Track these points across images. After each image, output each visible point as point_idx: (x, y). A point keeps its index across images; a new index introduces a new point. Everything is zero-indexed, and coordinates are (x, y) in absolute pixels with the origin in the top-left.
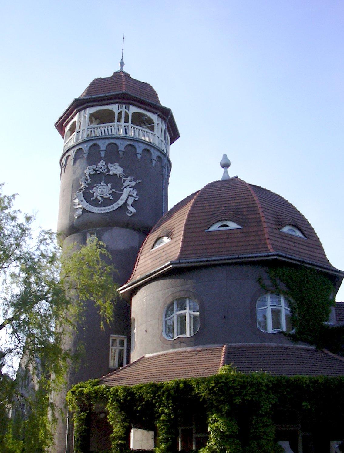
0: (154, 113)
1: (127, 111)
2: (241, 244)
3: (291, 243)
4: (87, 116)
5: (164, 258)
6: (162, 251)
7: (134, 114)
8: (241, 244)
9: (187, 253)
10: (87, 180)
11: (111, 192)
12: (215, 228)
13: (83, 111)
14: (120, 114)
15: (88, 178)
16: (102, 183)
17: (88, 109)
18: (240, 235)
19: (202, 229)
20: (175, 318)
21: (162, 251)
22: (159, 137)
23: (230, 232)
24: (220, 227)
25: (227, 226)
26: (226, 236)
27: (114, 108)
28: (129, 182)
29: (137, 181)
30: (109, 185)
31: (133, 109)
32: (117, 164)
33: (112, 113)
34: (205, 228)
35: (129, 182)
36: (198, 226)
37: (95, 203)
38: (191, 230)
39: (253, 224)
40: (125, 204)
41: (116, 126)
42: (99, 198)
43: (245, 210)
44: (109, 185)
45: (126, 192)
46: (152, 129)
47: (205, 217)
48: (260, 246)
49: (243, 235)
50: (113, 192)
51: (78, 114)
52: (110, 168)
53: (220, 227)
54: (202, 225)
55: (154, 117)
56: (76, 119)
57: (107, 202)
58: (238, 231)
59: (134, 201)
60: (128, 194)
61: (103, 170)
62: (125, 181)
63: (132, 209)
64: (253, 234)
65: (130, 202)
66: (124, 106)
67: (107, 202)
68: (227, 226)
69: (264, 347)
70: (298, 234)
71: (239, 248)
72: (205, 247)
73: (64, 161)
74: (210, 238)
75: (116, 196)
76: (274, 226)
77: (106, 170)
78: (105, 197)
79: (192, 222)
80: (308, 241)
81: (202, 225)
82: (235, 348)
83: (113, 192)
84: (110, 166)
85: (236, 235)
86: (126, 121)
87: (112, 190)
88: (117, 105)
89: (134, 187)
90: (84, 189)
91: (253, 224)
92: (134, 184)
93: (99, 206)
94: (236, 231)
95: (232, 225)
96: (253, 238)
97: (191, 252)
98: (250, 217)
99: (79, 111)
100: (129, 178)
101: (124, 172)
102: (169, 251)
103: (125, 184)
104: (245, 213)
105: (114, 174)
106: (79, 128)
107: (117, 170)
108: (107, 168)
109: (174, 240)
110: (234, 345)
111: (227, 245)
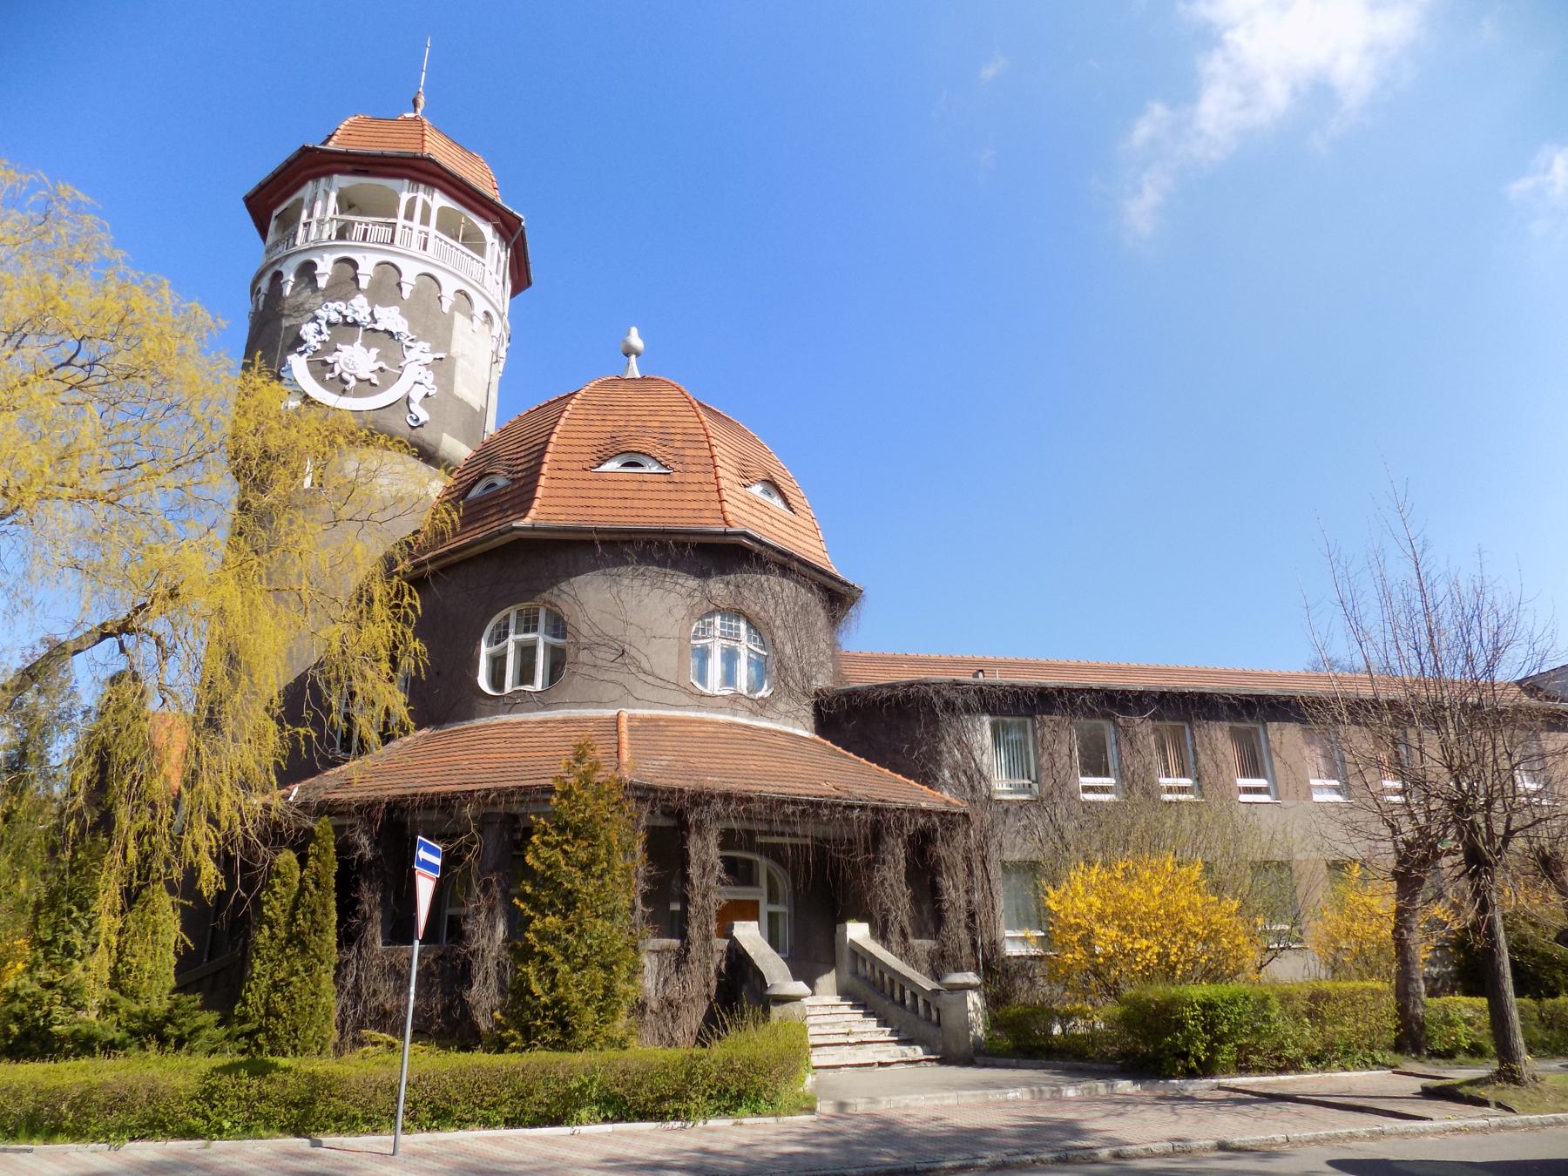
0: (487, 219)
1: (428, 200)
2: (666, 505)
3: (766, 518)
7: (442, 210)
8: (666, 505)
10: (320, 333)
11: (376, 367)
12: (612, 466)
13: (323, 180)
14: (411, 204)
15: (324, 328)
16: (358, 344)
17: (336, 177)
19: (586, 465)
22: (494, 270)
23: (647, 477)
26: (635, 486)
28: (419, 354)
29: (438, 356)
30: (374, 351)
31: (439, 201)
32: (395, 310)
34: (593, 464)
36: (576, 457)
39: (694, 468)
42: (345, 376)
43: (678, 437)
45: (412, 372)
46: (481, 250)
47: (591, 442)
48: (707, 514)
49: (671, 487)
50: (381, 369)
51: (310, 183)
54: (583, 457)
55: (487, 230)
56: (306, 192)
57: (367, 386)
59: (427, 396)
60: (415, 378)
61: (363, 316)
64: (695, 487)
65: (417, 395)
66: (422, 186)
67: (367, 386)
69: (702, 722)
70: (777, 502)
71: (661, 513)
73: (264, 285)
74: (600, 485)
75: (386, 377)
76: (735, 479)
77: (369, 319)
78: (361, 376)
79: (562, 449)
80: (796, 518)
82: (643, 720)
83: (381, 369)
84: (379, 311)
85: (656, 486)
86: (425, 220)
88: (406, 182)
90: (310, 353)
91: (694, 468)
92: (429, 358)
96: (690, 496)
97: (556, 510)
98: (688, 452)
99: (316, 177)
100: (421, 345)
104: (677, 444)
105: (386, 331)
106: (310, 215)
107: (390, 318)
108: (372, 314)
110: (639, 712)
111: (636, 503)
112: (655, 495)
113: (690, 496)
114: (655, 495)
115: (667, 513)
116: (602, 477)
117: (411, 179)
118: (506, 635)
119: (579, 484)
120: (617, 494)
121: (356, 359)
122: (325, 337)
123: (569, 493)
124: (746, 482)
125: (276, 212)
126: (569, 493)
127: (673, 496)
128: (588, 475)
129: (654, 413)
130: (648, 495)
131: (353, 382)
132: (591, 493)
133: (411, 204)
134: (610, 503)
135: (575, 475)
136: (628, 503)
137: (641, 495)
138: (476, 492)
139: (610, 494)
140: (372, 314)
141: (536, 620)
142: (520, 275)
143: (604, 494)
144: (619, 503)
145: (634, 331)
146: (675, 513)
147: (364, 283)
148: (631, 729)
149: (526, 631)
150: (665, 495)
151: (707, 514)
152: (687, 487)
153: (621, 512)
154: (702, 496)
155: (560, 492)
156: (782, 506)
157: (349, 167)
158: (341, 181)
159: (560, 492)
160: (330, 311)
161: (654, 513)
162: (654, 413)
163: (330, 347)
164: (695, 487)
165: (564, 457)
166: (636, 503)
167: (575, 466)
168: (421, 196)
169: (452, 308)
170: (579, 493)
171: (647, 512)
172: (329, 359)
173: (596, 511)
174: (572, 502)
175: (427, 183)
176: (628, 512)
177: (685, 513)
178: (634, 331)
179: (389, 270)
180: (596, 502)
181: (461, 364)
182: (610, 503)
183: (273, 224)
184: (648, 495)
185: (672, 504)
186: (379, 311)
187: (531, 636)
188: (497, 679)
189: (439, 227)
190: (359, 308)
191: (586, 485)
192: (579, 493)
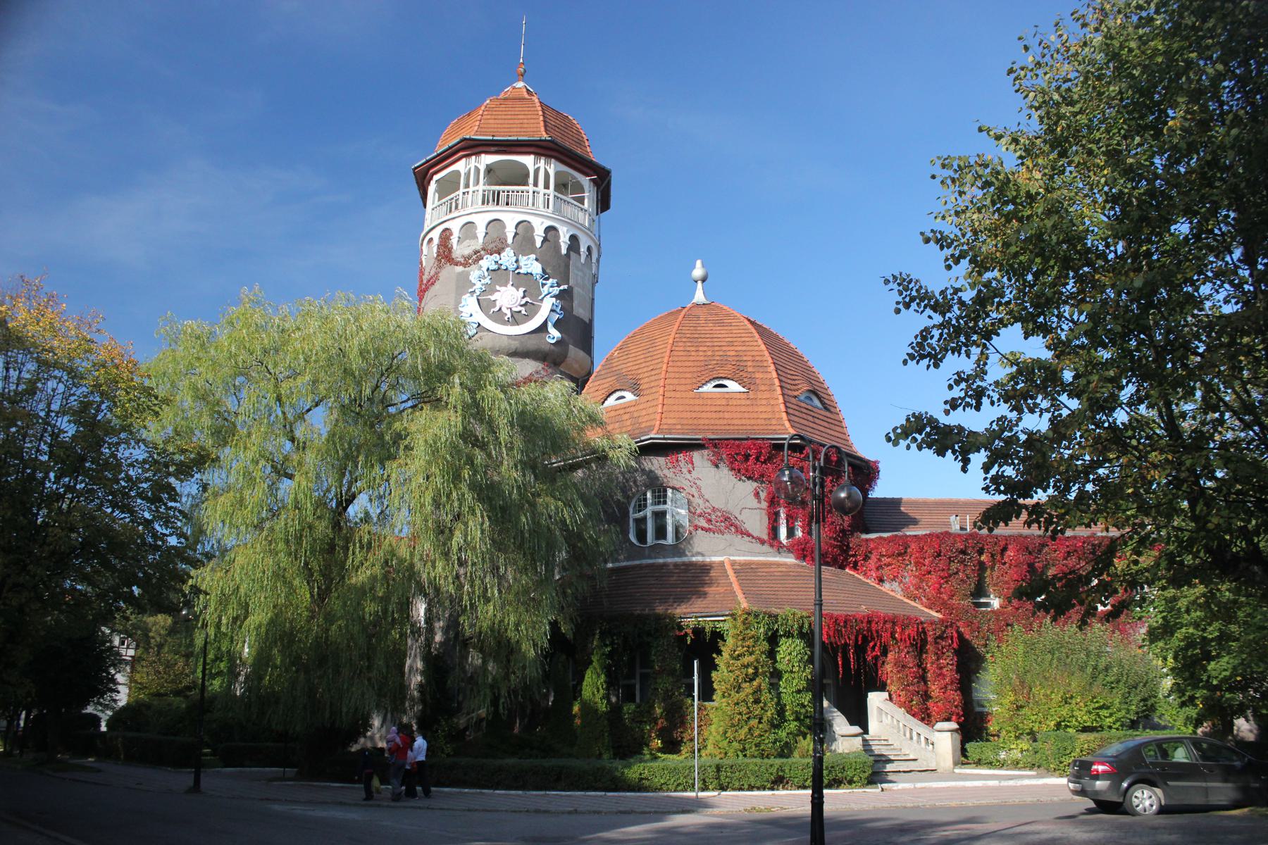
2: (746, 415)
4: (482, 168)
5: (629, 423)
6: (622, 412)
7: (557, 174)
8: (746, 415)
9: (670, 421)
12: (709, 388)
14: (537, 171)
18: (743, 402)
20: (649, 515)
21: (622, 412)
24: (716, 386)
25: (724, 386)
27: (528, 160)
32: (533, 256)
33: (524, 168)
35: (550, 288)
36: (683, 381)
37: (498, 317)
38: (672, 388)
39: (763, 388)
40: (545, 323)
41: (531, 194)
42: (504, 310)
43: (749, 364)
44: (522, 290)
46: (581, 201)
49: (748, 402)
52: (522, 264)
53: (716, 386)
54: (688, 381)
55: (585, 181)
56: (461, 166)
57: (516, 319)
58: (745, 396)
62: (543, 285)
63: (554, 334)
64: (764, 402)
68: (724, 386)
70: (817, 402)
71: (744, 422)
72: (694, 415)
75: (531, 309)
79: (672, 375)
80: (828, 414)
81: (688, 381)
82: (740, 564)
84: (523, 260)
85: (739, 402)
86: (547, 187)
87: (527, 299)
88: (532, 157)
89: (555, 296)
91: (763, 388)
92: (556, 291)
93: (507, 323)
94: (738, 396)
95: (733, 386)
96: (763, 409)
101: (544, 270)
102: (636, 415)
103: (545, 290)
104: (750, 369)
106: (467, 186)
108: (517, 261)
109: (644, 399)
111: (727, 415)
112: (738, 409)
113: (763, 409)
114: (738, 409)
115: (748, 422)
116: (701, 396)
117: (535, 154)
118: (645, 506)
119: (687, 402)
120: (714, 409)
121: (509, 297)
122: (487, 281)
123: (681, 408)
124: (796, 393)
125: (436, 177)
126: (681, 408)
127: (750, 409)
128: (691, 394)
129: (731, 344)
130: (734, 409)
131: (509, 315)
132: (697, 408)
133: (537, 171)
134: (709, 415)
135: (684, 395)
136: (721, 415)
137: (729, 408)
138: (611, 401)
139: (708, 409)
140: (517, 261)
141: (665, 496)
142: (603, 203)
143: (704, 408)
144: (714, 415)
145: (699, 263)
146: (753, 422)
147: (510, 241)
148: (736, 572)
149: (659, 503)
150: (743, 409)
151: (774, 422)
152: (759, 402)
153: (717, 422)
154: (769, 409)
155: (675, 408)
156: (819, 405)
157: (493, 149)
158: (488, 159)
159: (675, 408)
160: (488, 262)
161: (739, 422)
162: (731, 344)
163: (489, 289)
164: (764, 402)
165: (676, 381)
166: (727, 415)
167: (683, 388)
168: (542, 163)
169: (569, 249)
170: (688, 408)
171: (735, 422)
172: (493, 298)
173: (702, 422)
174: (684, 415)
175: (547, 156)
176: (721, 422)
177: (759, 422)
178: (699, 263)
179: (524, 229)
180: (699, 415)
181: (576, 290)
182: (709, 415)
183: (432, 188)
184: (734, 409)
185: (751, 416)
186: (523, 260)
187: (661, 507)
188: (642, 536)
189: (557, 188)
190: (507, 258)
191: (692, 402)
192: (688, 408)
